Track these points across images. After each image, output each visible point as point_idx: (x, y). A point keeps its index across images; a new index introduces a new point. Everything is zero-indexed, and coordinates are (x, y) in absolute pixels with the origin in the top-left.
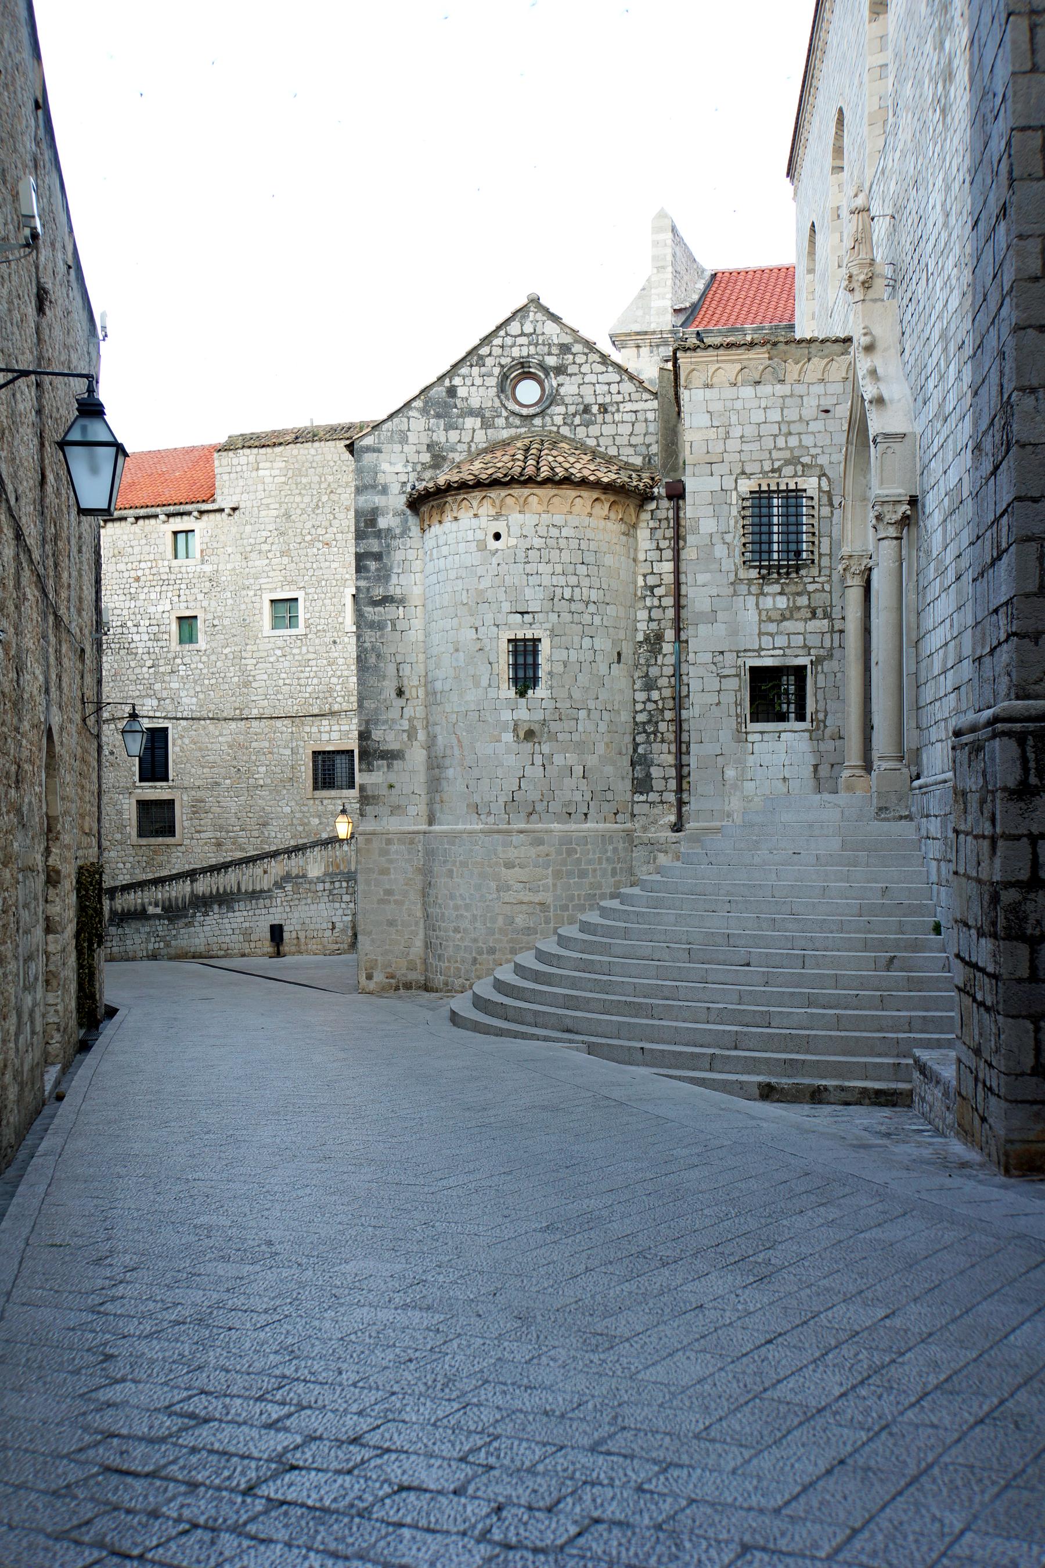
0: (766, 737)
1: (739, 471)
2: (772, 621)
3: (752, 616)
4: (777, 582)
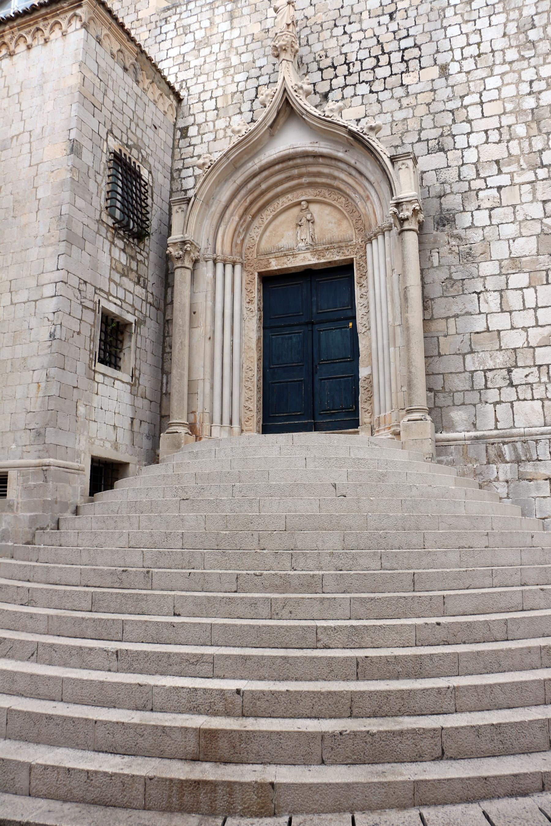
0: (107, 381)
1: (109, 128)
2: (118, 272)
3: (105, 259)
4: (122, 238)
